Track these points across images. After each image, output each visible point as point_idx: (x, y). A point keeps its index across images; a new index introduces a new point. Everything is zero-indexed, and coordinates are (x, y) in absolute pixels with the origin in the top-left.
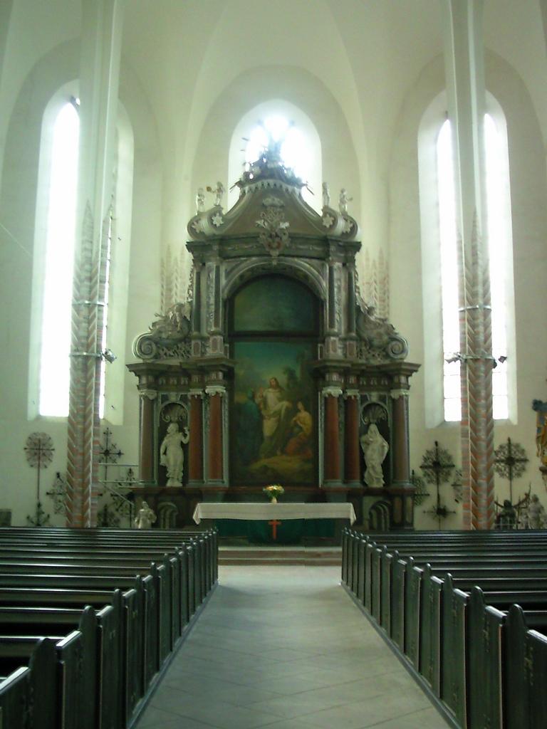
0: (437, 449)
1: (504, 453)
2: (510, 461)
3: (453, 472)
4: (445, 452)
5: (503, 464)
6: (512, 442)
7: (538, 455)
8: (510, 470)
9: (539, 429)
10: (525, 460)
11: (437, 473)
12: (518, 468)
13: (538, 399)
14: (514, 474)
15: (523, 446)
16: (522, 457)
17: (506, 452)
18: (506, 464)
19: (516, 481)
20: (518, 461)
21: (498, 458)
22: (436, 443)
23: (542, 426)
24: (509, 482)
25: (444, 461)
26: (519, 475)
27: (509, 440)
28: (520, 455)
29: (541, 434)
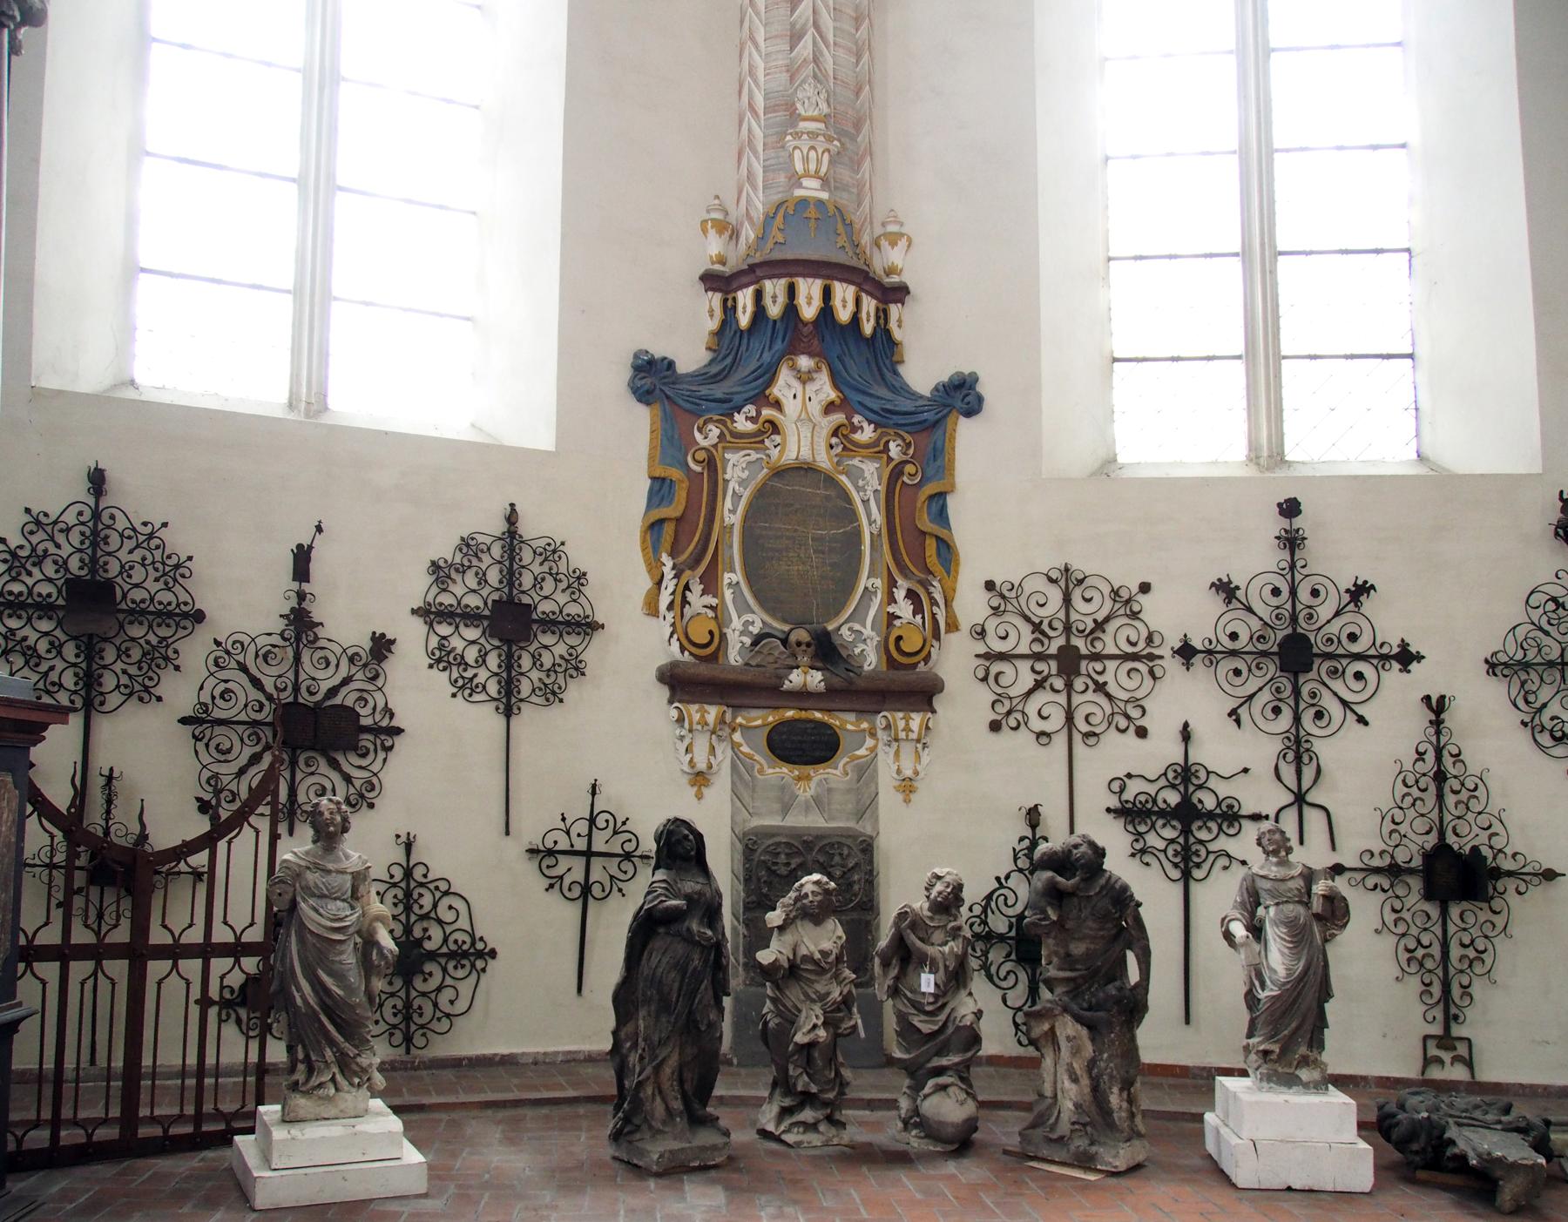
0: (96, 515)
1: (483, 580)
2: (511, 622)
3: (195, 651)
4: (149, 537)
5: (472, 633)
6: (526, 529)
7: (652, 609)
8: (509, 663)
9: (660, 488)
10: (587, 627)
11: (90, 648)
12: (547, 660)
13: (659, 350)
14: (525, 688)
15: (578, 557)
16: (573, 609)
17: (493, 576)
18: (491, 632)
19: (530, 719)
20: (549, 624)
21: (447, 599)
22: (97, 480)
23: (675, 473)
24: (503, 720)
25: (144, 588)
26: (551, 695)
27: (512, 518)
28: (562, 598)
29: (674, 510)
